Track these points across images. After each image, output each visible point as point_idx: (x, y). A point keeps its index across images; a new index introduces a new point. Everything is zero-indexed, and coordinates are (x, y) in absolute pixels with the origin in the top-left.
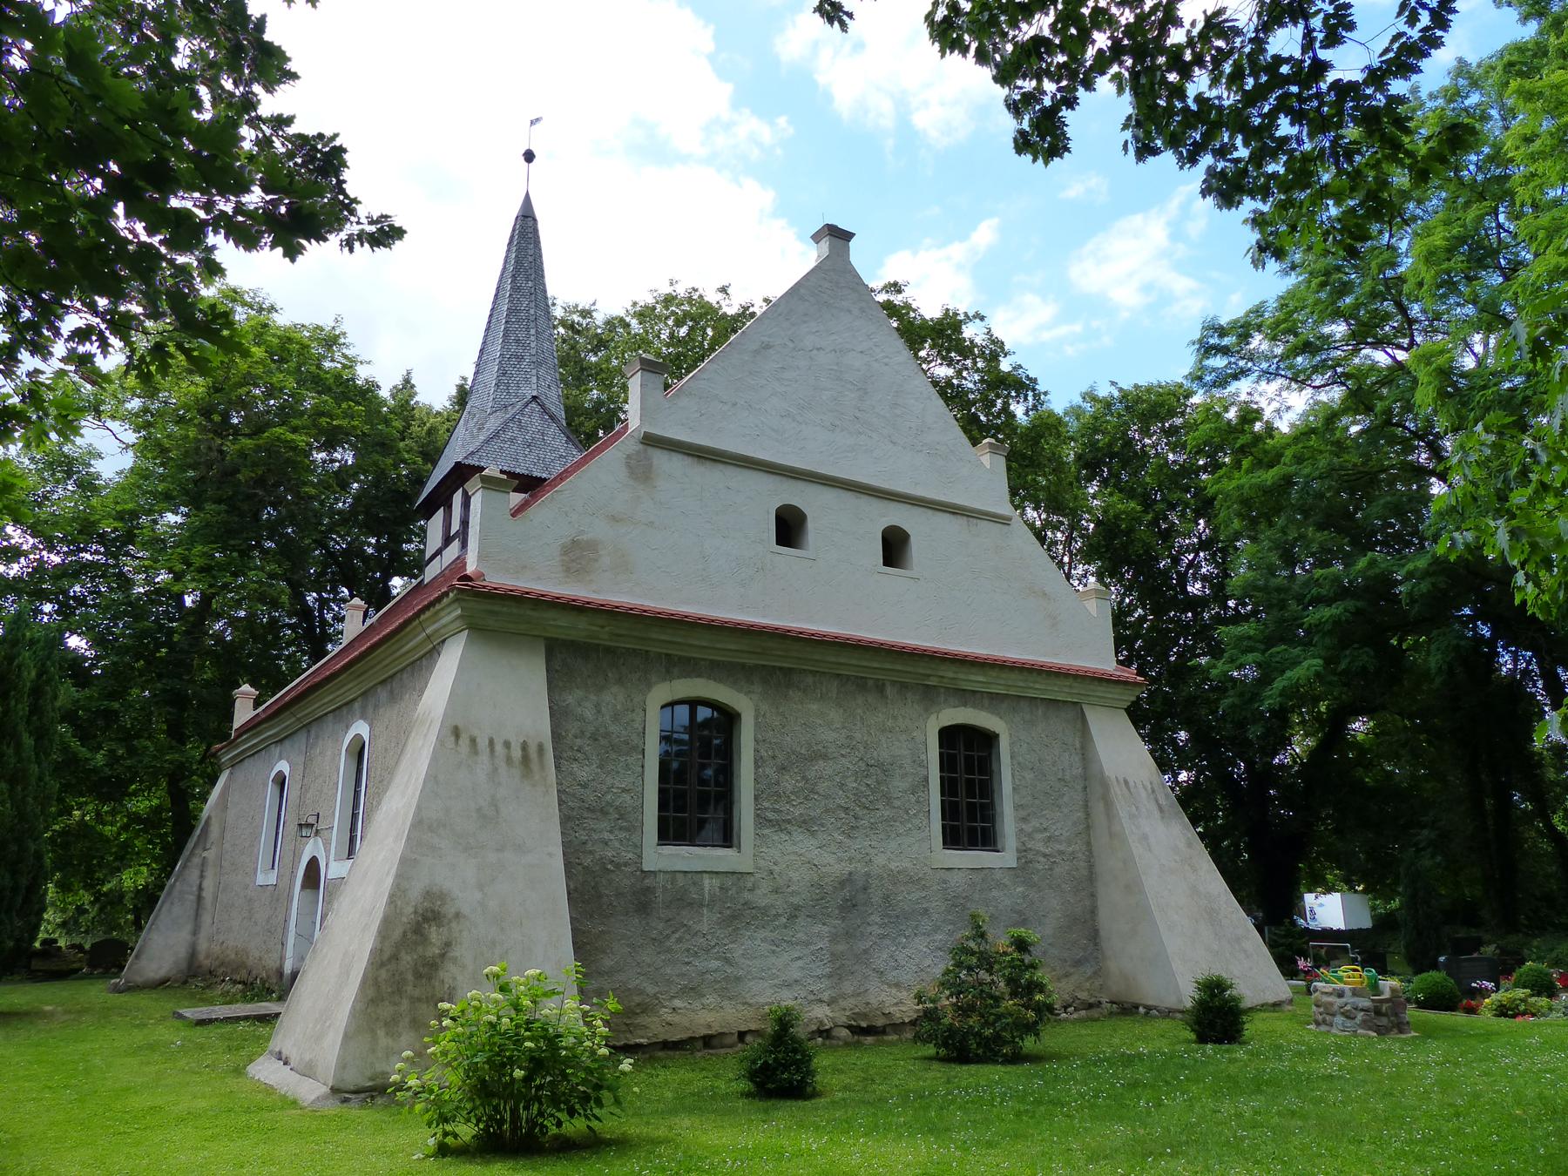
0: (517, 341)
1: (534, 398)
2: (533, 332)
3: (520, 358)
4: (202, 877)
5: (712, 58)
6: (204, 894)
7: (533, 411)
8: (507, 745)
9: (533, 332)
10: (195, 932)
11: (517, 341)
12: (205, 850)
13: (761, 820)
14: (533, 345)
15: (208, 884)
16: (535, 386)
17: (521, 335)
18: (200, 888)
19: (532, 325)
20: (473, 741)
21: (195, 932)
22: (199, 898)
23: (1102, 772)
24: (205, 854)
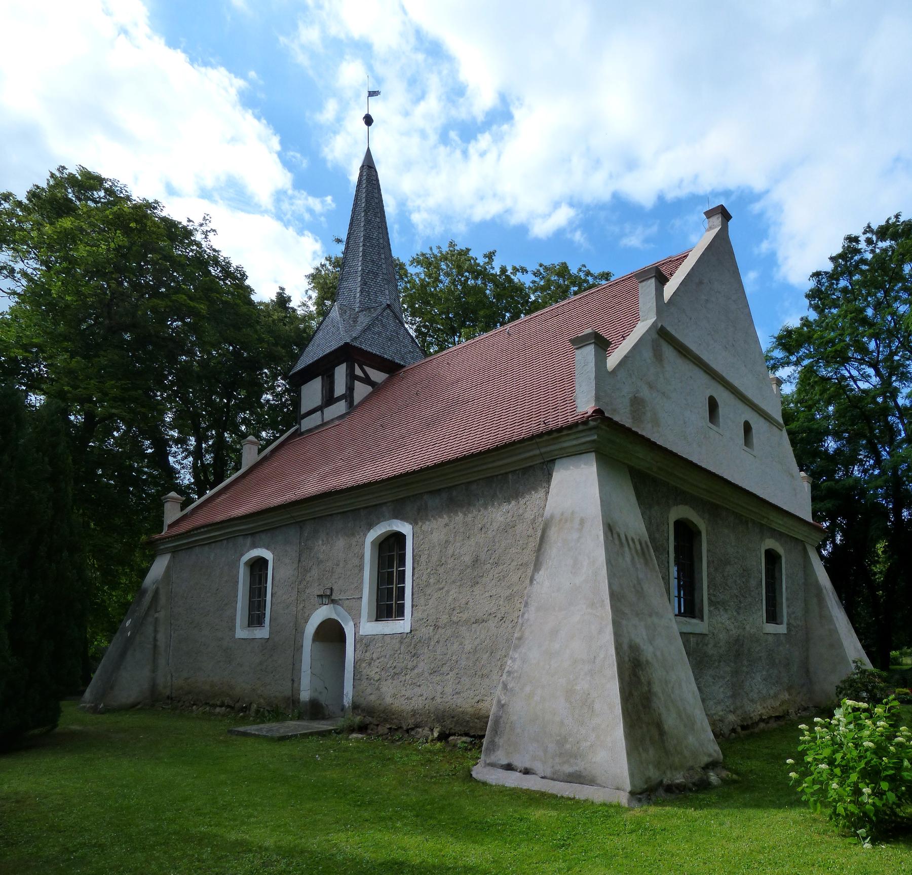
0: (373, 261)
1: (388, 306)
2: (383, 256)
3: (376, 275)
4: (156, 631)
5: (279, 155)
6: (158, 643)
7: (388, 315)
8: (633, 540)
9: (383, 256)
10: (154, 670)
11: (373, 261)
12: (156, 612)
13: (711, 603)
14: (384, 266)
15: (161, 636)
16: (388, 297)
17: (375, 258)
18: (155, 640)
19: (382, 251)
20: (619, 536)
21: (154, 670)
22: (155, 647)
23: (817, 581)
24: (157, 615)
